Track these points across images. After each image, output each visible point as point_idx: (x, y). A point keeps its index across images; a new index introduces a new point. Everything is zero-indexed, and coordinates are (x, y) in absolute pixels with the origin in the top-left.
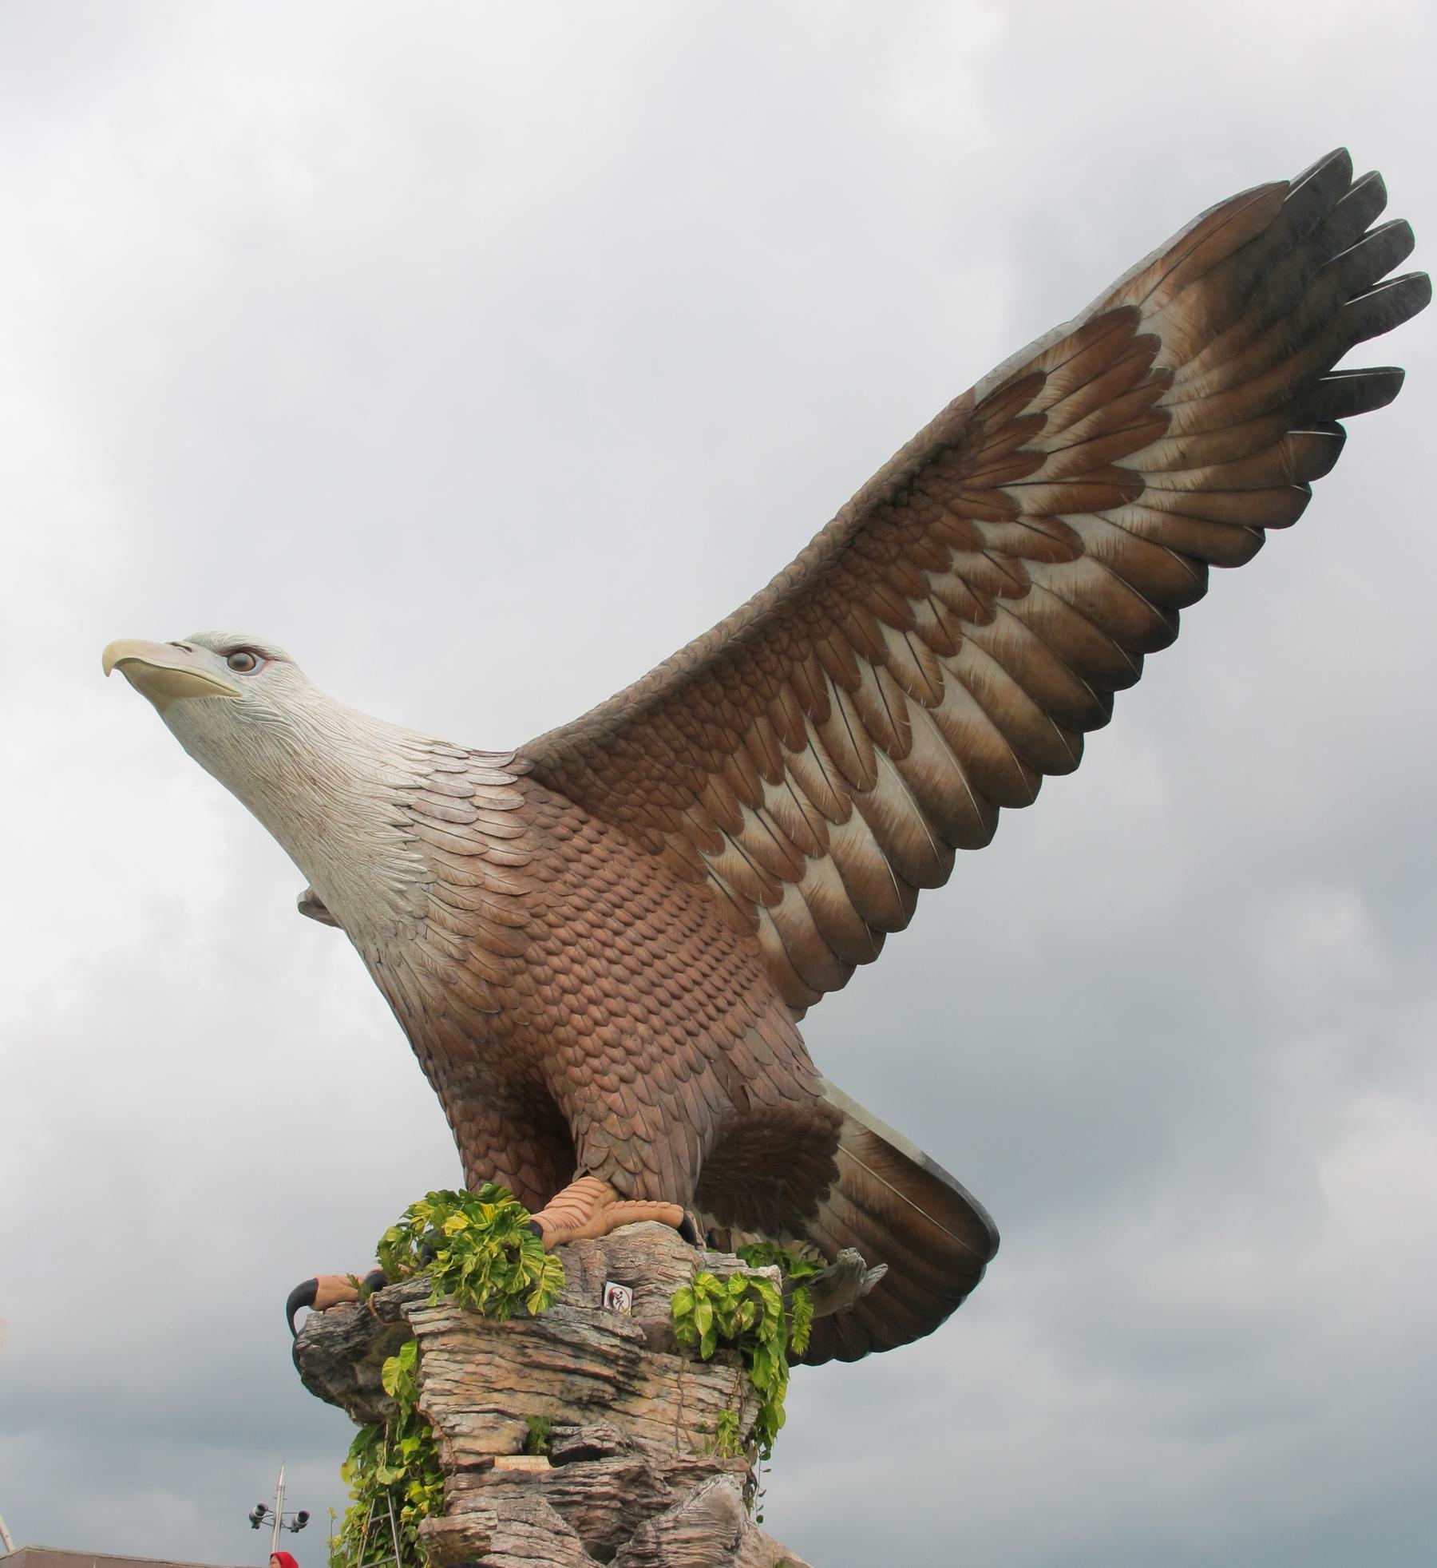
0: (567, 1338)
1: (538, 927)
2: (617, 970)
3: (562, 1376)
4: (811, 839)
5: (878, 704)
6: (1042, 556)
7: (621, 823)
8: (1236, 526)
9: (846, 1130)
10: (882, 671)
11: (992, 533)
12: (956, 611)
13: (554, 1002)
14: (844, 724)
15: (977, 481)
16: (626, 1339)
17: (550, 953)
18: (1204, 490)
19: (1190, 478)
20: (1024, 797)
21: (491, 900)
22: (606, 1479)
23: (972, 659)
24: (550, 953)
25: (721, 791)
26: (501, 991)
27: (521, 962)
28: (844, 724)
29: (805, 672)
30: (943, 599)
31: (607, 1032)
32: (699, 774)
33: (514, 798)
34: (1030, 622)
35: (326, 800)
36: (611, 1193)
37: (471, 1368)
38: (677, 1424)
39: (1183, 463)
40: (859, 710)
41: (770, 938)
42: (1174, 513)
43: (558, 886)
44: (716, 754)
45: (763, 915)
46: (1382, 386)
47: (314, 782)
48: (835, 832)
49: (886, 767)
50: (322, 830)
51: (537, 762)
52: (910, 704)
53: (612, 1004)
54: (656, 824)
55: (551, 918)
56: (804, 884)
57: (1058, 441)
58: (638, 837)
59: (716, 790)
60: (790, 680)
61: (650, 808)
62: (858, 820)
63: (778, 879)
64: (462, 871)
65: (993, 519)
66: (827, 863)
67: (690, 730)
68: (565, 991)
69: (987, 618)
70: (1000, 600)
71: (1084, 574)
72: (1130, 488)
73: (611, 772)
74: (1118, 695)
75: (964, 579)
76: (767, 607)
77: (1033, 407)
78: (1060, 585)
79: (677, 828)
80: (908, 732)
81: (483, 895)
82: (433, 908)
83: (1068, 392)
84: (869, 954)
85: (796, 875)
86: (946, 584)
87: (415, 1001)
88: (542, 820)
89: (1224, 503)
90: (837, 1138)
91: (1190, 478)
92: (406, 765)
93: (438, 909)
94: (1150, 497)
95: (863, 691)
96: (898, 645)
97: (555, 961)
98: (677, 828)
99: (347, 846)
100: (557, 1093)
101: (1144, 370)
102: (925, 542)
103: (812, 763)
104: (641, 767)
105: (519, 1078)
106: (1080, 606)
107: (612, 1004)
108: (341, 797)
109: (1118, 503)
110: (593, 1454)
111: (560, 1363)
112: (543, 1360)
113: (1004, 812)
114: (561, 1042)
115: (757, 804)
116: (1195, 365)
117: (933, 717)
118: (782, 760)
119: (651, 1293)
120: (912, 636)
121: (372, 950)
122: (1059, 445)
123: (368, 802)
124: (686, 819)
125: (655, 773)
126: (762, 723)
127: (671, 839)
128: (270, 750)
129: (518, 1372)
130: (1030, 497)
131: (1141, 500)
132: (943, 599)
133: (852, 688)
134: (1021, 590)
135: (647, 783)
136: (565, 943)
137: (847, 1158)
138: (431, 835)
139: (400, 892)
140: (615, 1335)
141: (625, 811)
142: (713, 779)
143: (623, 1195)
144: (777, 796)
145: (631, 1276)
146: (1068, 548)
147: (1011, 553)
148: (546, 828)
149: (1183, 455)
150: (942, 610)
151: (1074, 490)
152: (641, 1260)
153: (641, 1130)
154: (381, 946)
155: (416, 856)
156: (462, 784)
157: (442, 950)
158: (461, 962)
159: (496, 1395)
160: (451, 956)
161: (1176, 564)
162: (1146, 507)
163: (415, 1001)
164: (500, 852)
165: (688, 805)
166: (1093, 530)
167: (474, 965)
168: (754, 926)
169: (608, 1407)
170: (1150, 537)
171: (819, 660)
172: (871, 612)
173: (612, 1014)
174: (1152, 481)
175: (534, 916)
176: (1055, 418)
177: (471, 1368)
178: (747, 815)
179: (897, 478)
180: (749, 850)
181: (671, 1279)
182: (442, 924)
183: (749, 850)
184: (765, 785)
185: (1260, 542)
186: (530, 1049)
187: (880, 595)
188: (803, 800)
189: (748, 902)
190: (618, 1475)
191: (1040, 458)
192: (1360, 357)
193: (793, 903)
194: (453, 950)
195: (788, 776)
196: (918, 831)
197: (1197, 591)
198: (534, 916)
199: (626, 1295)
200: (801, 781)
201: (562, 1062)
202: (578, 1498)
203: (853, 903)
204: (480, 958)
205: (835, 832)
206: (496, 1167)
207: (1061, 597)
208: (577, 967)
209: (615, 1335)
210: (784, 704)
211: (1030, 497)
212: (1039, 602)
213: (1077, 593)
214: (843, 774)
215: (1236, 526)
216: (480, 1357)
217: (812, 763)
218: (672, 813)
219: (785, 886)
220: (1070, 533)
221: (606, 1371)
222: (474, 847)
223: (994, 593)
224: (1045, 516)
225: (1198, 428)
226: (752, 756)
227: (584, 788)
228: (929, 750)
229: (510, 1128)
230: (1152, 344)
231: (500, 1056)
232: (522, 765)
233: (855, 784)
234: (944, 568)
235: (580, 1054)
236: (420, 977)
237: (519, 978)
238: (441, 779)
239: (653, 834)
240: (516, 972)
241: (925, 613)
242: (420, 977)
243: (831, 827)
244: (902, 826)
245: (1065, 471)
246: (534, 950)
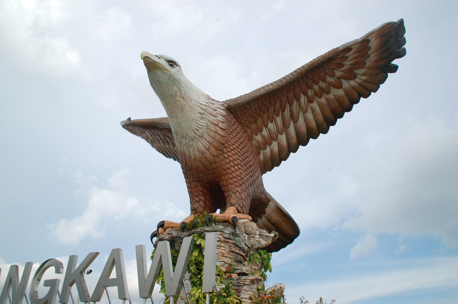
0: (240, 246)
1: (226, 145)
2: (240, 158)
3: (236, 254)
4: (275, 137)
5: (295, 110)
6: (335, 87)
7: (241, 124)
8: (368, 90)
9: (271, 204)
10: (297, 103)
11: (329, 79)
12: (316, 94)
13: (229, 164)
14: (287, 113)
15: (331, 67)
16: (249, 247)
17: (228, 152)
18: (366, 81)
19: (364, 78)
20: (315, 137)
21: (218, 136)
22: (248, 281)
23: (315, 105)
24: (228, 152)
25: (261, 122)
26: (216, 158)
27: (222, 152)
28: (287, 113)
29: (284, 99)
30: (314, 90)
31: (238, 173)
32: (258, 117)
33: (224, 113)
34: (328, 100)
35: (184, 103)
36: (237, 211)
37: (220, 250)
38: (251, 268)
39: (364, 74)
40: (291, 110)
41: (261, 156)
42: (359, 84)
43: (231, 136)
44: (262, 113)
45: (262, 152)
46: (394, 69)
47: (184, 98)
48: (280, 136)
49: (292, 124)
50: (182, 110)
52: (300, 111)
53: (239, 166)
54: (247, 126)
55: (230, 143)
56: (271, 146)
58: (243, 128)
59: (260, 121)
60: (281, 100)
61: (247, 122)
62: (284, 135)
63: (267, 144)
64: (213, 128)
65: (330, 76)
66: (276, 143)
67: (260, 106)
68: (231, 161)
69: (320, 97)
70: (324, 94)
71: (340, 92)
72: (354, 77)
73: (242, 112)
74: (338, 119)
75: (320, 88)
76: (284, 83)
77: (347, 55)
78: (335, 93)
79: (250, 128)
80: (298, 117)
81: (217, 135)
82: (204, 135)
84: (278, 165)
85: (270, 144)
86: (316, 87)
87: (193, 156)
88: (229, 119)
89: (367, 84)
90: (268, 205)
91: (364, 78)
92: (204, 100)
93: (205, 135)
94: (357, 80)
95: (293, 106)
96: (303, 98)
97: (229, 154)
98: (250, 128)
99: (188, 116)
100: (223, 185)
101: (366, 53)
102: (317, 77)
103: (279, 120)
104: (248, 111)
105: (213, 180)
106: (338, 99)
107: (239, 166)
108: (189, 103)
109: (351, 79)
110: (245, 274)
111: (237, 251)
112: (234, 250)
113: (311, 139)
114: (227, 173)
115: (266, 126)
116: (374, 55)
117: (304, 115)
118: (273, 118)
119: (253, 237)
120: (306, 97)
121: (184, 142)
122: (348, 64)
123: (195, 106)
124: (252, 126)
125: (251, 114)
126: (272, 108)
127: (249, 130)
128: (175, 88)
129: (228, 252)
130: (338, 73)
131: (355, 80)
132: (314, 90)
133: (291, 106)
134: (328, 93)
135: (248, 116)
136: (232, 150)
137: (269, 210)
138: (207, 118)
139: (197, 130)
140: (247, 246)
141: (242, 121)
142: (260, 118)
143: (239, 212)
144: (271, 125)
145: (248, 232)
146: (339, 86)
147: (330, 84)
148: (230, 122)
149: (365, 73)
150: (313, 93)
151: (345, 74)
152: (250, 229)
153: (244, 197)
154: (187, 141)
155: (204, 122)
156: (215, 106)
157: (204, 146)
158: (208, 150)
159: (224, 258)
160: (206, 148)
161: (356, 95)
162: (356, 82)
163: (193, 156)
164: (221, 125)
165: (254, 123)
166: (345, 84)
167: (211, 151)
168: (259, 153)
169: (241, 263)
170: (354, 88)
171: (287, 97)
172: (301, 90)
173: (239, 169)
174: (358, 77)
175: (227, 142)
176: (350, 58)
177: (220, 250)
178: (264, 128)
179: (319, 62)
180: (263, 136)
181: (255, 234)
182: (206, 140)
183: (263, 136)
184: (269, 122)
185: (370, 94)
186: (219, 173)
187: (304, 86)
188: (275, 128)
189: (260, 148)
190: (251, 280)
191: (343, 65)
192: (395, 62)
193: (268, 150)
194: (207, 146)
196: (294, 140)
197: (357, 102)
198: (227, 142)
199: (247, 236)
200: (276, 123)
201: (227, 178)
202: (242, 284)
203: (279, 153)
204: (212, 149)
205: (280, 136)
206: (200, 200)
207: (335, 96)
208: (234, 156)
209: (247, 246)
210: (278, 106)
211: (338, 73)
212: (331, 96)
213: (338, 96)
214: (284, 123)
215: (368, 90)
216: (222, 248)
217: (279, 120)
218: (250, 123)
219: (267, 146)
220: (341, 83)
221: (244, 255)
222: (216, 123)
223: (323, 92)
224: (338, 78)
225: (369, 68)
226: (268, 115)
227: (237, 114)
228: (301, 122)
229: (205, 191)
230: (370, 48)
231: (211, 174)
232: (226, 105)
233: (286, 125)
234: (317, 84)
235: (232, 177)
236: (196, 151)
237: (221, 156)
238: (210, 104)
239: (246, 128)
241: (310, 93)
242: (196, 151)
243: (279, 135)
244: (292, 138)
245: (345, 70)
246: (225, 150)
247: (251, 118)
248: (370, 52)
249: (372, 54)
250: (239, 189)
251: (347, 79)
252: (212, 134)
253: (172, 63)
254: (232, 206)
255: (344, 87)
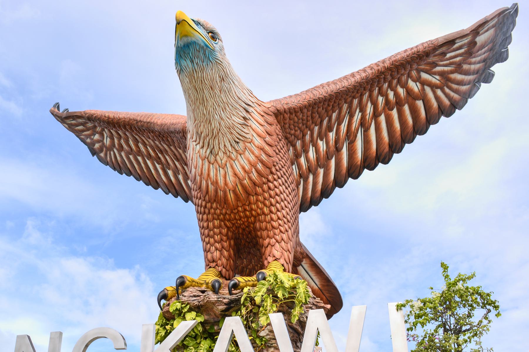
1: (273, 170)
24: (275, 180)
51: (278, 110)
55: (277, 167)
61: (293, 137)
104: (297, 121)
139: (238, 143)
195: (324, 140)
204: (254, 176)
235: (276, 218)
240: (264, 183)
246: (270, 177)
247: (299, 131)
250: (285, 236)
252: (257, 152)
253: (214, 35)
254: (276, 260)
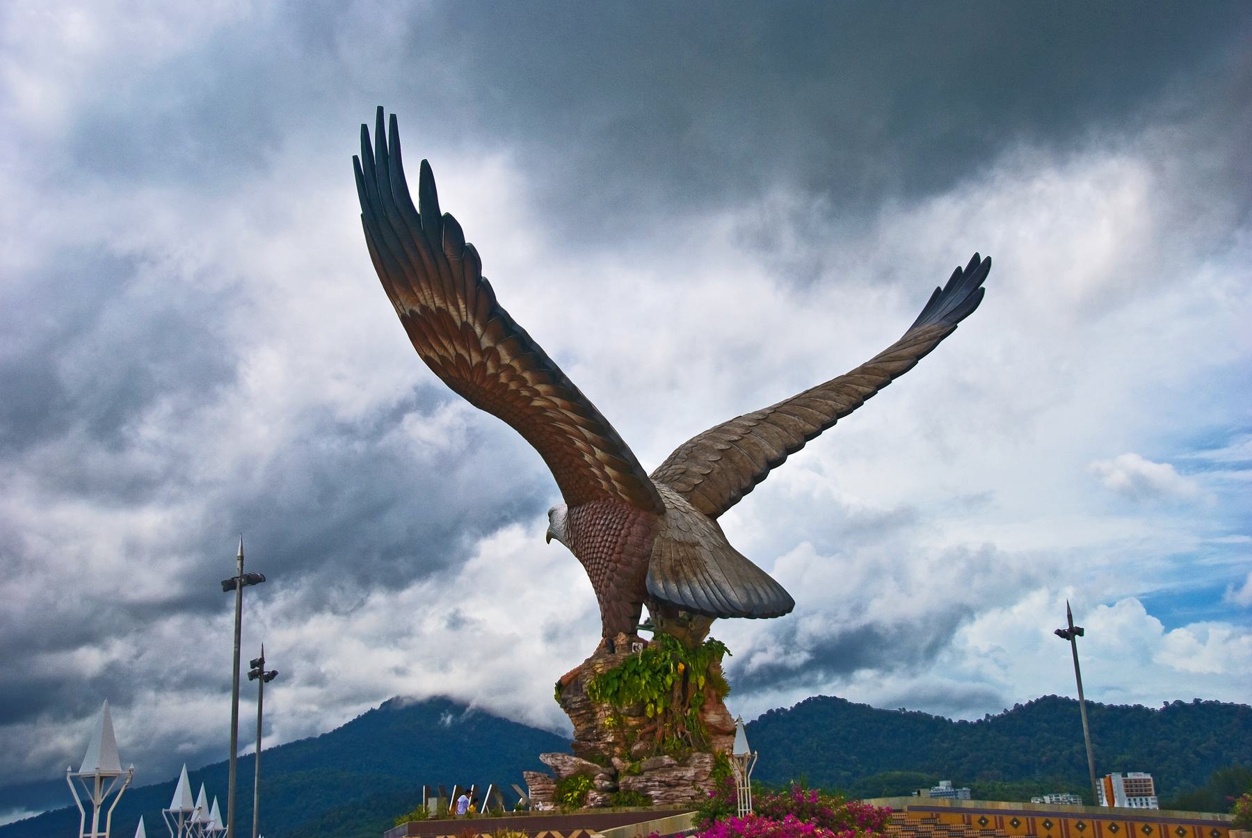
57: (451, 351)
65: (485, 370)
83: (432, 348)
130: (476, 359)
166: (486, 342)
170: (485, 327)
191: (459, 356)
245: (464, 347)
248: (417, 309)
249: (418, 301)
251: (477, 342)
255: (491, 345)
